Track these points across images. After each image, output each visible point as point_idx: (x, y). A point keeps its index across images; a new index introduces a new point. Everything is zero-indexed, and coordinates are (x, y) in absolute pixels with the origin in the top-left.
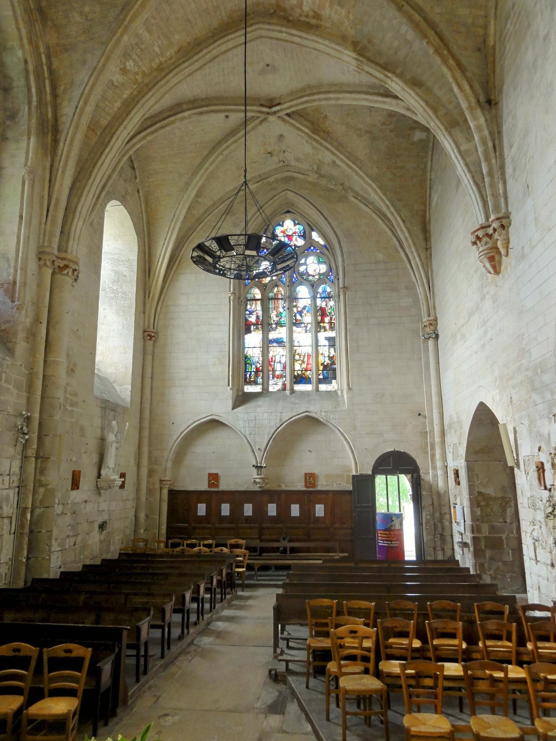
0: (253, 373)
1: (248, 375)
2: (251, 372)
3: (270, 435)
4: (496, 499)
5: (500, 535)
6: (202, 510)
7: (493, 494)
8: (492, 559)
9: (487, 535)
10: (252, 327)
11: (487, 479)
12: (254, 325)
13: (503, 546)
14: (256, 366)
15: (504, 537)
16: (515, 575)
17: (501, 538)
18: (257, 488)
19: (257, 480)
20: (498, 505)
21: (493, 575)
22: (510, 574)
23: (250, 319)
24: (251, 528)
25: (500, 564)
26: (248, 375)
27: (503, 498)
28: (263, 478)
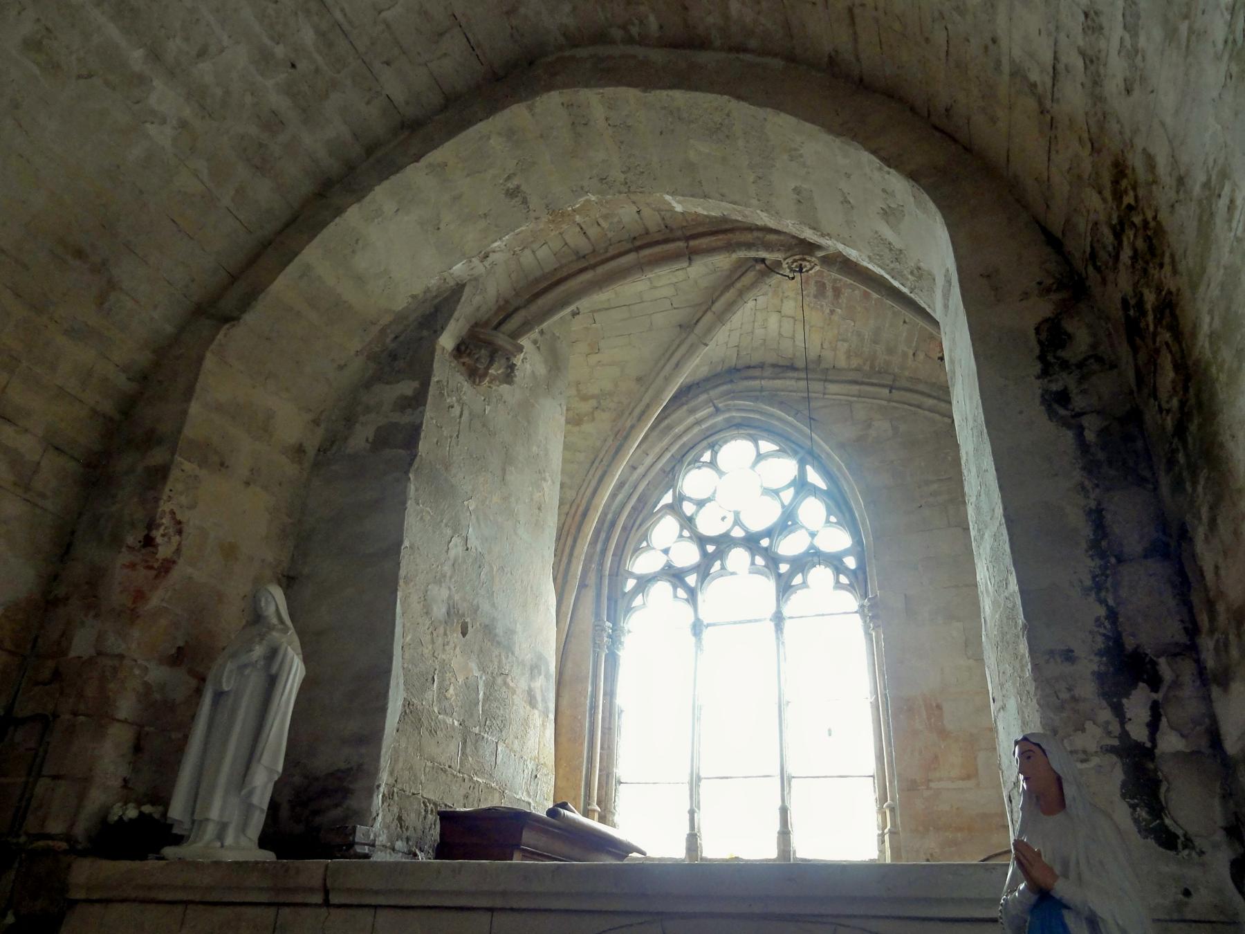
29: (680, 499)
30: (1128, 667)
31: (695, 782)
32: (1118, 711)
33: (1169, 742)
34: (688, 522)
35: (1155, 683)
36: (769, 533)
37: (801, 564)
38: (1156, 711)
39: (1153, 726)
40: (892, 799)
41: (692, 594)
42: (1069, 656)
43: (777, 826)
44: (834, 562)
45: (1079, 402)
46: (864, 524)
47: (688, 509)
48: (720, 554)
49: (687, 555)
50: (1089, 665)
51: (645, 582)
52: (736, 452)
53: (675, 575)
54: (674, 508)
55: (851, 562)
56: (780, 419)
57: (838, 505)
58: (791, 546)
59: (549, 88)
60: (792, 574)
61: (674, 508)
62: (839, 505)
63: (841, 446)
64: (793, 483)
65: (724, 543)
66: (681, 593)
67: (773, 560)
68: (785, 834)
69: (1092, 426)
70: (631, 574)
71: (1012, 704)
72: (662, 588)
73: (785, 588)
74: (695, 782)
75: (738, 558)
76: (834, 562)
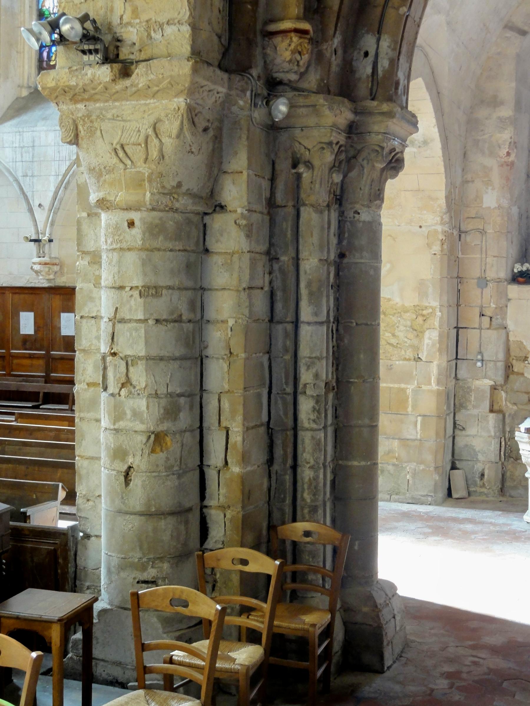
1: (45, 54)
3: (60, 178)
5: (403, 386)
6: (27, 324)
13: (406, 408)
15: (410, 388)
16: (422, 467)
17: (403, 391)
18: (41, 282)
19: (37, 267)
20: (409, 323)
22: (413, 465)
24: (31, 357)
25: (396, 443)
26: (45, 54)
28: (46, 264)
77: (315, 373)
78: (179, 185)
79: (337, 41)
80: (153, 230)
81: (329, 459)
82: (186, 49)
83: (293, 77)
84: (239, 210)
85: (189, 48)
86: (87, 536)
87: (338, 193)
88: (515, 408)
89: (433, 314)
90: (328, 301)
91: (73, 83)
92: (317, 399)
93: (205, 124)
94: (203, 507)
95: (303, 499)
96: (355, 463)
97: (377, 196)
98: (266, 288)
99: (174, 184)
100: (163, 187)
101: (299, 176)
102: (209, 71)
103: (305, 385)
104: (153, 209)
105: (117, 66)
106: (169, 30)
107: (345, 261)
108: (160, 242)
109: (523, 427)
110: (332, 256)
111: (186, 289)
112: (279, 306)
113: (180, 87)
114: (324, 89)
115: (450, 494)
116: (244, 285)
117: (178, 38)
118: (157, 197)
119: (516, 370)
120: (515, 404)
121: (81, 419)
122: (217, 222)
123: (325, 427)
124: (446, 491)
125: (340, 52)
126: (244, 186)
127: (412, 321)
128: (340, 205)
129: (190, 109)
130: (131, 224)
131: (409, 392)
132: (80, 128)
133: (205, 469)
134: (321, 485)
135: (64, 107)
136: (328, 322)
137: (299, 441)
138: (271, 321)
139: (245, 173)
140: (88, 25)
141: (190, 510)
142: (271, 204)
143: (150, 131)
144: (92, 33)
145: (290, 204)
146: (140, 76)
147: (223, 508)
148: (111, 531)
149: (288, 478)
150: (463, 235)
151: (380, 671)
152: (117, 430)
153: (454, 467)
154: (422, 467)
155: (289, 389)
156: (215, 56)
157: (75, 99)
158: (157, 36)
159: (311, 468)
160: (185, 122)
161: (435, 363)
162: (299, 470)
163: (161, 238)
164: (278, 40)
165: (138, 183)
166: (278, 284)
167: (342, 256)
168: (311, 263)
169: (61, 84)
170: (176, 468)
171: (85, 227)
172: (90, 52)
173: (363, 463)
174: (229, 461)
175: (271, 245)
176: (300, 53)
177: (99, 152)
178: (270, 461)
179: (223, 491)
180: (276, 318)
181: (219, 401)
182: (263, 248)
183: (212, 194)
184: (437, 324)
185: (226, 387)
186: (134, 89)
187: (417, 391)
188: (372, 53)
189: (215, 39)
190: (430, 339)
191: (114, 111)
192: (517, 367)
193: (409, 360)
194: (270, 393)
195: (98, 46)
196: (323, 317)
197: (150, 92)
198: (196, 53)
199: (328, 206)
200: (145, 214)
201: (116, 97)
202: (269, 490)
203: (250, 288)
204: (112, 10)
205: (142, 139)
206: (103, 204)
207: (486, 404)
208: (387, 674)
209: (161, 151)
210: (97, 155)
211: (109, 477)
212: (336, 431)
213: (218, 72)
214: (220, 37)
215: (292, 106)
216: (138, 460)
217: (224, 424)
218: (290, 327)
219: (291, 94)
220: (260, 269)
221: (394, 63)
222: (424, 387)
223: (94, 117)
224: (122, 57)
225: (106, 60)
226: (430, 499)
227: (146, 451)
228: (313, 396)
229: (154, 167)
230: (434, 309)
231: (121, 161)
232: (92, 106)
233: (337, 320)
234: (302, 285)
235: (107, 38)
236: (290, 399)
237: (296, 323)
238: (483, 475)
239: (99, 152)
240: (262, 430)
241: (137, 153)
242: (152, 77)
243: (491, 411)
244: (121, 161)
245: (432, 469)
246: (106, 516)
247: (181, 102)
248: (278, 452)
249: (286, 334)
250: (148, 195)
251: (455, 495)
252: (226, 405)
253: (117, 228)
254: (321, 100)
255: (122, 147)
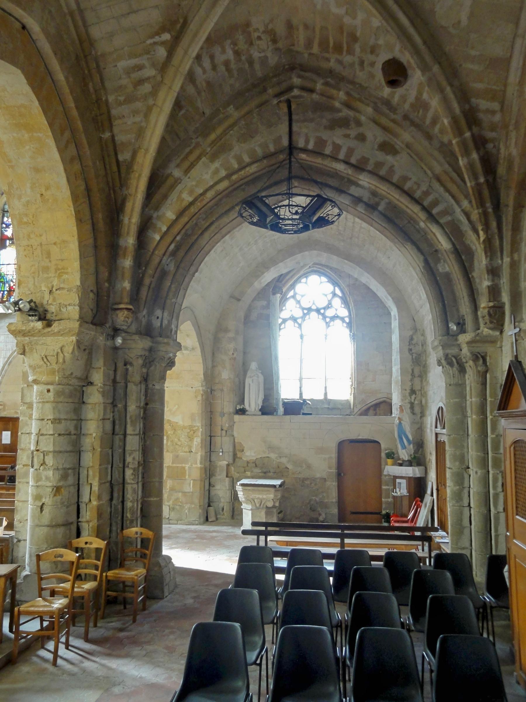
0: (6, 292)
2: (4, 291)
3: (6, 359)
4: (184, 427)
5: (184, 465)
7: (181, 423)
8: (172, 489)
9: (171, 464)
10: (8, 241)
11: (177, 406)
12: (10, 239)
13: (185, 477)
14: (10, 285)
15: (187, 466)
16: (193, 506)
17: (184, 468)
20: (186, 434)
21: (171, 506)
23: (6, 233)
25: (180, 494)
27: (191, 427)
29: (295, 294)
30: (413, 392)
31: (301, 380)
32: (411, 398)
33: (416, 402)
34: (298, 302)
35: (416, 394)
36: (324, 308)
37: (333, 318)
38: (415, 398)
39: (415, 400)
40: (355, 385)
41: (300, 326)
42: (406, 390)
43: (324, 392)
44: (342, 319)
45: (413, 351)
46: (353, 310)
47: (298, 297)
48: (308, 314)
49: (298, 313)
50: (408, 391)
51: (284, 321)
52: (314, 279)
53: (294, 319)
54: (294, 297)
55: (347, 320)
56: (329, 273)
57: (345, 302)
58: (330, 313)
59: (315, 250)
60: (330, 322)
61: (294, 297)
62: (345, 301)
63: (348, 286)
64: (332, 293)
65: (310, 310)
66: (296, 325)
67: (324, 317)
68: (326, 394)
69: (414, 355)
70: (280, 318)
71: (396, 393)
72: (290, 323)
73: (328, 325)
74: (301, 380)
75: (314, 314)
76: (342, 319)
77: (133, 458)
78: (72, 374)
79: (145, 312)
80: (58, 394)
81: (139, 497)
82: (77, 316)
83: (125, 328)
84: (99, 385)
85: (78, 316)
86: (19, 541)
87: (145, 377)
88: (238, 475)
89: (198, 429)
90: (140, 424)
91: (24, 328)
92: (134, 470)
93: (84, 348)
94: (78, 522)
95: (127, 517)
96: (152, 499)
97: (163, 378)
98: (111, 419)
99: (70, 373)
100: (64, 375)
101: (127, 370)
102: (87, 325)
103: (129, 463)
104: (59, 384)
105: (45, 322)
106: (69, 308)
107: (148, 406)
108: (61, 399)
109: (238, 483)
110: (142, 404)
111: (74, 420)
112: (117, 427)
113: (74, 332)
114: (139, 333)
115: (207, 519)
116: (101, 418)
117: (74, 311)
118: (61, 379)
119: (238, 456)
120: (238, 473)
121: (19, 482)
122: (90, 389)
123: (138, 483)
124: (205, 518)
125: (146, 316)
126: (102, 374)
127: (188, 433)
128: (146, 382)
129: (78, 341)
130: (48, 391)
131: (187, 468)
132: (26, 348)
133: (80, 504)
134: (135, 509)
135: (19, 339)
136: (139, 434)
137: (125, 490)
138: (113, 434)
139: (102, 368)
140: (32, 304)
141: (72, 523)
142: (114, 381)
143: (59, 351)
144: (34, 308)
145: (123, 381)
146: (55, 327)
147: (88, 522)
148: (32, 536)
149: (120, 507)
150: (213, 392)
151: (162, 598)
152: (37, 486)
153: (209, 506)
154: (193, 506)
155: (121, 465)
156: (89, 318)
157: (24, 335)
158: (64, 310)
159: (131, 501)
160: (76, 347)
161: (199, 454)
162: (125, 503)
163: (62, 397)
164: (118, 312)
165: (53, 372)
166: (117, 417)
167: (147, 404)
168: (132, 408)
169: (18, 329)
170: (66, 503)
171: (25, 391)
172: (33, 315)
173: (155, 499)
174: (92, 499)
175: (114, 400)
176: (128, 318)
177: (35, 358)
178: (111, 499)
179: (88, 513)
180: (116, 433)
181: (88, 471)
182: (110, 401)
183: (87, 377)
184: (200, 434)
185: (91, 464)
186: (53, 332)
187: (190, 468)
188: (160, 317)
189: (90, 312)
190: (196, 442)
191: (42, 341)
192: (239, 454)
193: (187, 452)
194: (112, 467)
195: (37, 313)
196: (137, 432)
197: (59, 333)
198: (82, 319)
199: (140, 383)
200: (55, 386)
201: (44, 335)
202: (111, 512)
203: (104, 419)
204: (43, 298)
205: (55, 354)
206: (35, 382)
207: (225, 473)
208: (165, 599)
209: (64, 359)
210: (33, 360)
211: (32, 509)
212: (143, 485)
213: (91, 326)
214: (92, 310)
215: (124, 340)
216: (47, 500)
217: (90, 482)
218: (122, 437)
219: (123, 335)
220: (108, 411)
221: (170, 323)
222: (194, 466)
223: (33, 343)
224: (47, 318)
225: (40, 319)
226: (197, 522)
227: (52, 496)
228: (132, 468)
229: (60, 366)
230: (198, 427)
231: (45, 363)
232: (32, 338)
233: (144, 433)
234: (128, 417)
235: (41, 310)
236: (121, 470)
237: (125, 435)
238: (223, 509)
239: (35, 358)
240: (108, 485)
241: (53, 360)
242: (61, 328)
243: (227, 477)
244: (45, 363)
245: (198, 507)
246: (30, 528)
247: (74, 338)
248: (115, 495)
249: (120, 440)
250: (57, 378)
251: (210, 520)
252: (91, 473)
253: (42, 392)
254: (136, 337)
255: (46, 357)
